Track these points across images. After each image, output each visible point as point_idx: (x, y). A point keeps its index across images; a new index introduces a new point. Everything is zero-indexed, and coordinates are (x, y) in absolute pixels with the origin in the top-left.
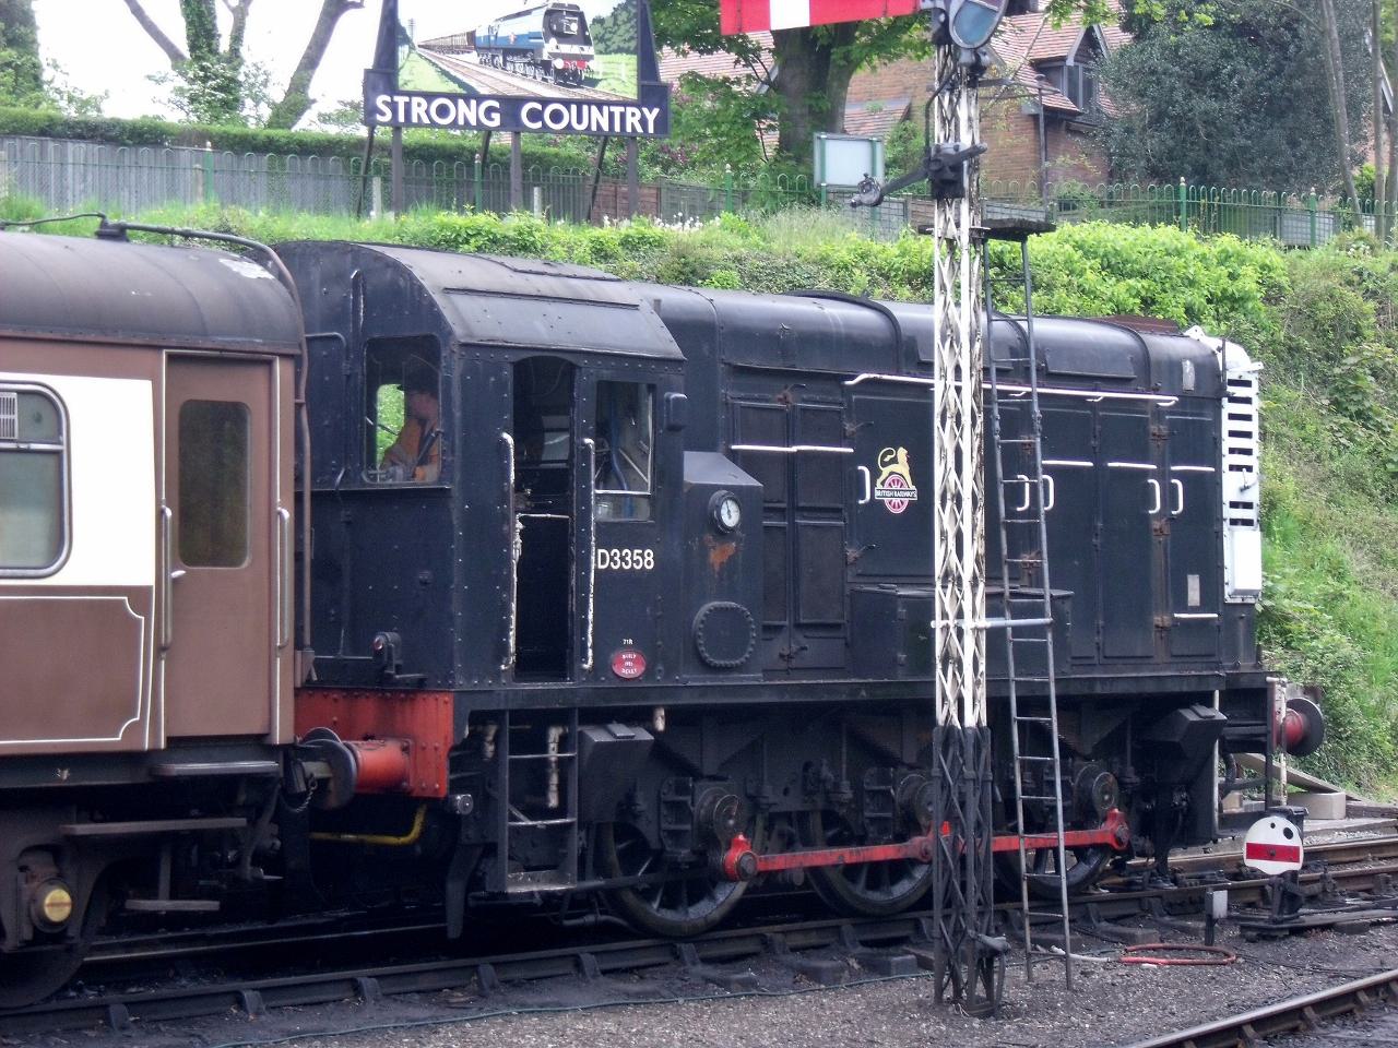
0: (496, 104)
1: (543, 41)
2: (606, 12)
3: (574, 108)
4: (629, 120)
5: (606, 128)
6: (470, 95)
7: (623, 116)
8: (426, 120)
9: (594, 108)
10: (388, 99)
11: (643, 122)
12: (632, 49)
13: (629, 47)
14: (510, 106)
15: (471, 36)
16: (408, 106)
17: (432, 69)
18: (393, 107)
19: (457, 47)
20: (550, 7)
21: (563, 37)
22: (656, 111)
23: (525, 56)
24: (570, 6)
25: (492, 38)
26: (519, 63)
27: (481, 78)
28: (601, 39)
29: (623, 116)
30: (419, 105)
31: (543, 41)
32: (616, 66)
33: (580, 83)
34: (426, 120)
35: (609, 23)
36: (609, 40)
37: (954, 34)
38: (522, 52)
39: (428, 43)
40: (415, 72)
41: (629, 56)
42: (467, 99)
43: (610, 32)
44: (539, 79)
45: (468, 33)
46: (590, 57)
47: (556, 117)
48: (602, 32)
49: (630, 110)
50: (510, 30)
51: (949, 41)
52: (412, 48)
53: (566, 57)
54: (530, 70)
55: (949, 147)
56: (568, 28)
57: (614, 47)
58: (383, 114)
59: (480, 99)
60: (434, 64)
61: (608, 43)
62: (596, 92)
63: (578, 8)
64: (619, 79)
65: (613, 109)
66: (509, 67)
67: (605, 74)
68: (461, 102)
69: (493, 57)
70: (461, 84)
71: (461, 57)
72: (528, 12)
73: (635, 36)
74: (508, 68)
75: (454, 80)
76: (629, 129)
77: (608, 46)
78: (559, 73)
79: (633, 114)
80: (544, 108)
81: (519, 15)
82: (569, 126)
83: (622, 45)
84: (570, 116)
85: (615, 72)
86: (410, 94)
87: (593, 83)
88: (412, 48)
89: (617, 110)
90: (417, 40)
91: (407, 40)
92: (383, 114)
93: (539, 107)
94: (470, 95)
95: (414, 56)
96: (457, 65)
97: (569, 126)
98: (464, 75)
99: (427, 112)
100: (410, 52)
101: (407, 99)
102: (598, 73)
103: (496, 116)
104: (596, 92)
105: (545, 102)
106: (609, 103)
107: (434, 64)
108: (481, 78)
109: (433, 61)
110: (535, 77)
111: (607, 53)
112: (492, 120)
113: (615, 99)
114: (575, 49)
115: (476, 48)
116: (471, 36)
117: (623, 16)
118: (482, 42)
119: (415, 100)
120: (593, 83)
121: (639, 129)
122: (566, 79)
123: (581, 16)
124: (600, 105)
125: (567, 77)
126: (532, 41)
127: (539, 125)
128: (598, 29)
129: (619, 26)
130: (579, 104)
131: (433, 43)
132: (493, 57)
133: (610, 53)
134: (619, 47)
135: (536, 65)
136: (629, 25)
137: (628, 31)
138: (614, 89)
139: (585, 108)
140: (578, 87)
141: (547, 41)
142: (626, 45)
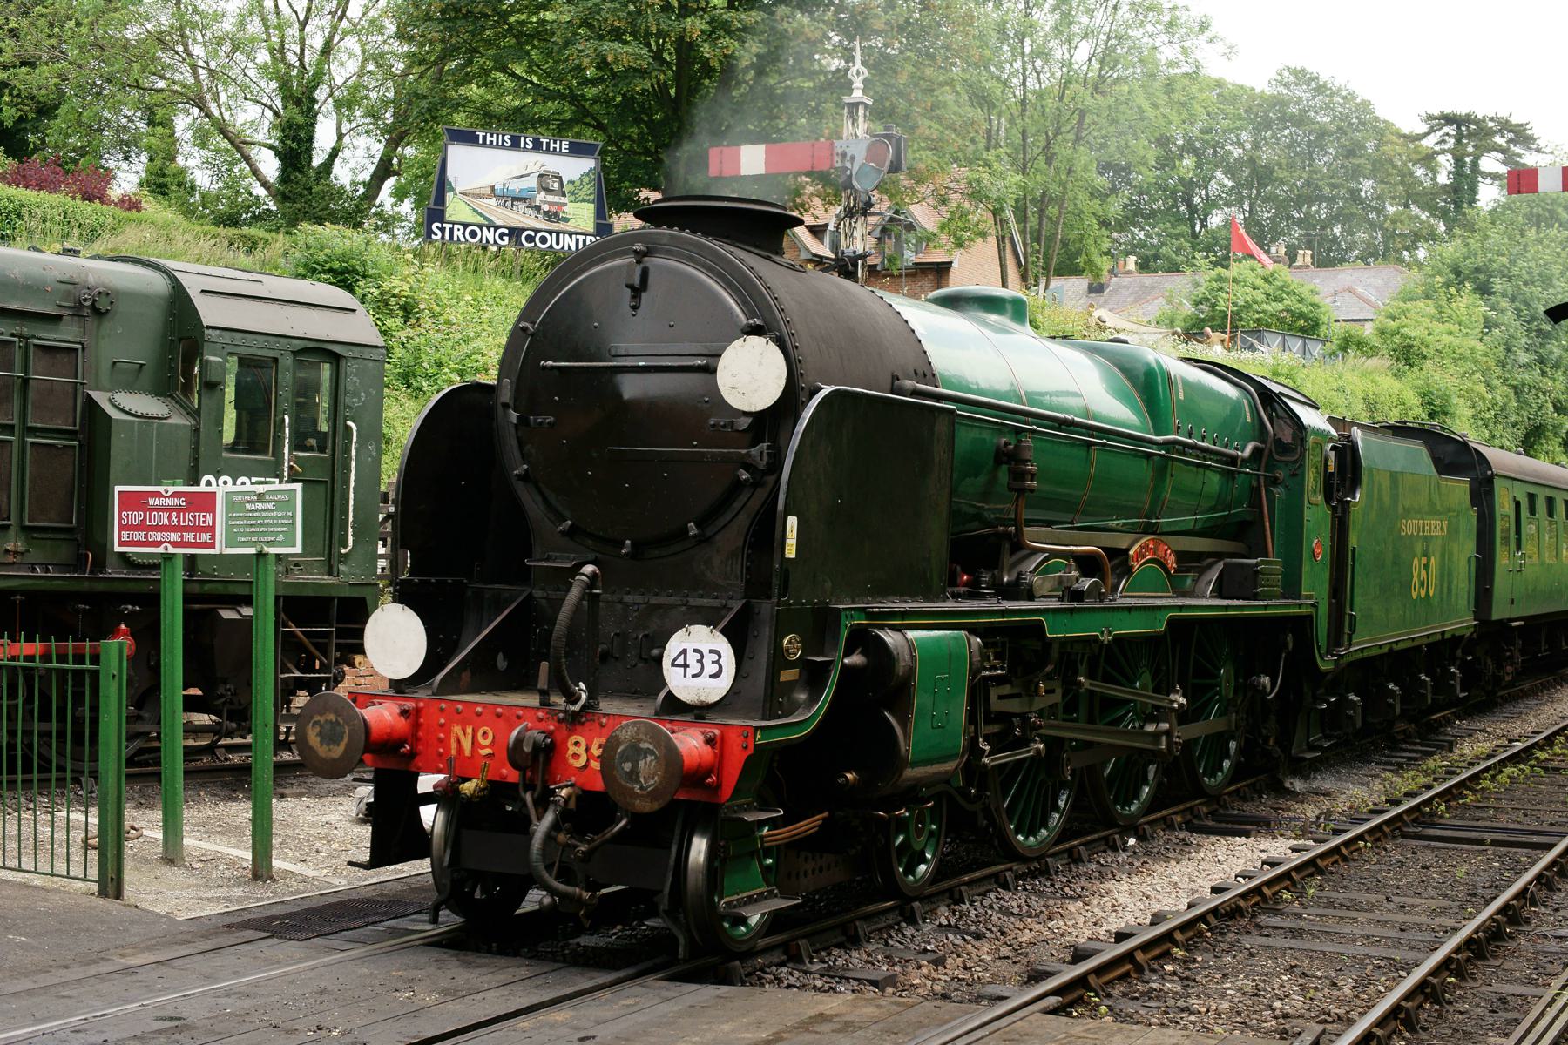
0: (506, 231)
2: (576, 178)
5: (573, 248)
6: (491, 226)
14: (515, 233)
15: (492, 188)
16: (452, 230)
18: (442, 230)
21: (548, 190)
26: (521, 206)
33: (558, 220)
34: (462, 239)
35: (578, 184)
37: (855, 183)
38: (524, 200)
40: (456, 209)
42: (489, 228)
47: (544, 240)
49: (589, 238)
50: (516, 187)
51: (852, 187)
53: (551, 204)
54: (528, 211)
55: (849, 252)
59: (496, 228)
70: (485, 218)
72: (528, 175)
78: (546, 213)
82: (551, 246)
84: (551, 240)
86: (454, 223)
87: (567, 220)
89: (581, 238)
90: (458, 190)
91: (452, 189)
94: (491, 226)
97: (551, 246)
103: (506, 238)
105: (537, 231)
114: (556, 199)
116: (492, 188)
117: (587, 180)
118: (498, 192)
119: (456, 227)
120: (567, 220)
123: (560, 178)
125: (551, 216)
130: (558, 233)
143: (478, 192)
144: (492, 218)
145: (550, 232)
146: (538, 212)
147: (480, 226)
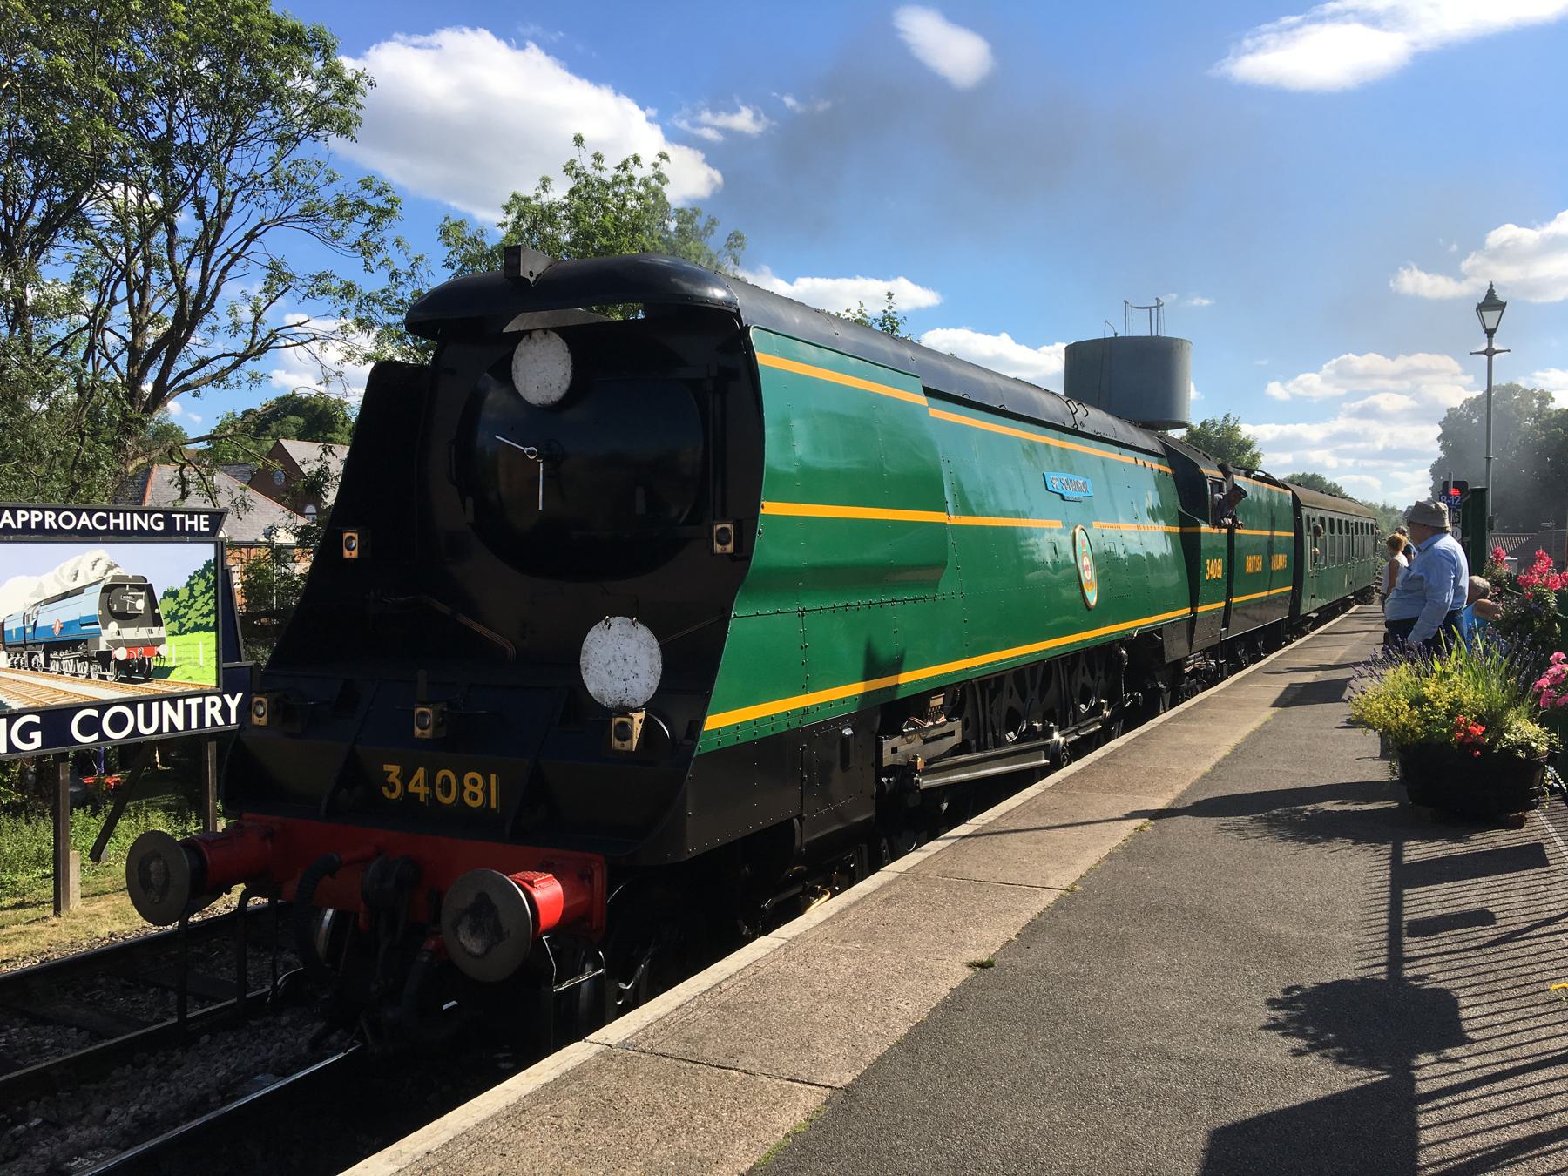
1: (100, 626)
2: (180, 583)
3: (140, 707)
4: (209, 711)
5: (180, 725)
7: (201, 707)
9: (166, 704)
11: (225, 711)
12: (211, 625)
13: (208, 623)
14: (54, 720)
20: (108, 581)
21: (125, 618)
22: (239, 696)
23: (76, 650)
25: (29, 631)
28: (174, 617)
29: (201, 707)
31: (100, 626)
32: (190, 648)
35: (184, 595)
36: (184, 616)
38: (72, 645)
43: (185, 607)
44: (95, 677)
46: (161, 641)
47: (118, 722)
49: (209, 700)
50: (54, 618)
53: (129, 644)
54: (83, 668)
56: (133, 607)
57: (191, 624)
61: (182, 620)
63: (146, 580)
64: (196, 664)
65: (188, 701)
66: (54, 666)
67: (178, 659)
69: (31, 656)
72: (79, 591)
74: (52, 668)
77: (182, 625)
78: (122, 666)
79: (213, 705)
80: (102, 715)
81: (66, 596)
83: (199, 621)
85: (192, 656)
87: (164, 672)
89: (194, 702)
93: (95, 713)
97: (135, 730)
102: (171, 659)
104: (168, 684)
105: (103, 706)
106: (185, 696)
108: (11, 687)
110: (89, 676)
111: (181, 634)
112: (32, 741)
114: (142, 633)
117: (201, 585)
120: (164, 672)
123: (149, 589)
124: (173, 700)
125: (134, 671)
126: (83, 628)
127: (95, 737)
130: (148, 703)
132: (31, 656)
133: (185, 633)
134: (195, 623)
135: (90, 660)
136: (207, 596)
137: (207, 603)
139: (155, 705)
141: (105, 627)
142: (204, 621)
146: (106, 667)
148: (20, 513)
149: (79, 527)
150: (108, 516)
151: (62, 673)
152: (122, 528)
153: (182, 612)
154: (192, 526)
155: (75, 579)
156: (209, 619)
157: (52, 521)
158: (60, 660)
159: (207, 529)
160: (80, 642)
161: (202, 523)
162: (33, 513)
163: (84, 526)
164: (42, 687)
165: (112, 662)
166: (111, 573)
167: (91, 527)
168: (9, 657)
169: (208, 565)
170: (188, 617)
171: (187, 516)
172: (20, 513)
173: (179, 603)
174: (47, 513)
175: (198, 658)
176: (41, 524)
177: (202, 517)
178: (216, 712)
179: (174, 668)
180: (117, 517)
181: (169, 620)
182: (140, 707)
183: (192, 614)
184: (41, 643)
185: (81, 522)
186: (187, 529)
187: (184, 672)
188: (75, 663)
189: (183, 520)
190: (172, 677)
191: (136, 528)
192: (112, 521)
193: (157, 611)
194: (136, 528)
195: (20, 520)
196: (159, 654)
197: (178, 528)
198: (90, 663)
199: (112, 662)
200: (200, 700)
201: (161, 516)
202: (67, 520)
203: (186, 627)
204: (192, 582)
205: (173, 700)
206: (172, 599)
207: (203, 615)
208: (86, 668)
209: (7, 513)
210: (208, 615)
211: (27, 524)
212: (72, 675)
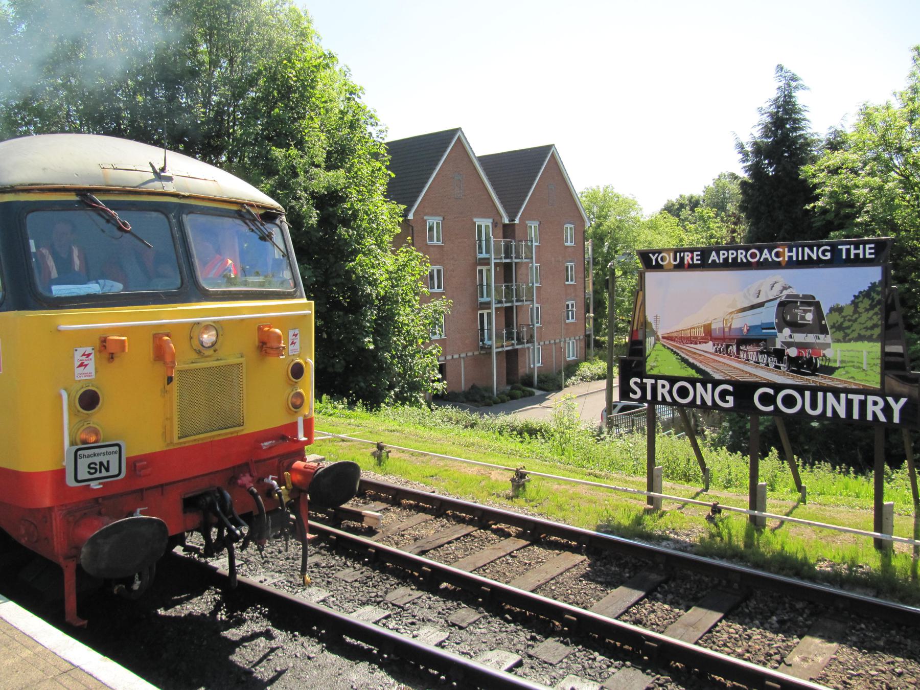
0: (730, 388)
2: (845, 300)
3: (807, 394)
4: (870, 408)
5: (842, 414)
6: (706, 380)
7: (863, 404)
8: (669, 399)
9: (829, 395)
10: (638, 380)
11: (887, 410)
12: (875, 337)
13: (872, 335)
17: (674, 357)
19: (695, 338)
20: (783, 299)
21: (796, 326)
24: (805, 296)
25: (726, 330)
26: (752, 351)
27: (715, 364)
28: (839, 328)
29: (863, 404)
30: (663, 386)
31: (776, 331)
34: (669, 399)
35: (849, 311)
36: (848, 328)
39: (670, 335)
41: (871, 344)
43: (849, 320)
44: (771, 367)
45: (705, 326)
47: (789, 401)
48: (841, 320)
49: (870, 399)
50: (742, 323)
52: (657, 339)
53: (800, 346)
54: (763, 358)
56: (803, 318)
57: (855, 335)
58: (635, 393)
59: (716, 383)
60: (675, 353)
61: (847, 331)
62: (832, 379)
63: (814, 298)
64: (859, 367)
65: (850, 396)
66: (743, 355)
67: (842, 362)
68: (698, 385)
70: (699, 370)
71: (698, 346)
72: (761, 305)
73: (879, 323)
74: (741, 356)
75: (693, 366)
76: (870, 417)
77: (846, 335)
78: (792, 361)
80: (776, 393)
81: (753, 307)
83: (863, 333)
86: (656, 378)
87: (830, 370)
88: (657, 339)
89: (856, 398)
90: (660, 334)
91: (654, 333)
92: (635, 393)
93: (771, 391)
95: (658, 346)
96: (695, 353)
98: (701, 362)
99: (670, 392)
100: (655, 343)
101: (653, 381)
103: (730, 398)
104: (832, 379)
105: (778, 388)
106: (847, 391)
107: (675, 353)
108: (715, 364)
109: (674, 350)
110: (767, 365)
111: (845, 342)
112: (727, 402)
113: (854, 387)
114: (810, 338)
115: (713, 339)
117: (867, 303)
118: (717, 334)
119: (660, 382)
121: (882, 418)
122: (800, 366)
123: (817, 305)
124: (836, 392)
126: (764, 331)
127: (771, 408)
128: (836, 317)
129: (860, 313)
130: (814, 390)
131: (674, 335)
132: (728, 346)
133: (849, 341)
134: (859, 335)
135: (769, 354)
136: (871, 312)
137: (871, 318)
138: (853, 378)
139: (820, 395)
140: (813, 374)
141: (780, 331)
142: (869, 333)
143: (687, 334)
144: (708, 370)
145: (801, 389)
146: (780, 360)
147: (693, 382)
148: (722, 252)
149: (761, 260)
150: (784, 251)
151: (748, 360)
152: (795, 259)
153: (846, 324)
154: (857, 255)
155: (758, 297)
156: (873, 332)
157: (743, 256)
158: (746, 352)
159: (699, 262)
160: (760, 340)
161: (868, 251)
162: (730, 252)
163: (766, 259)
164: (735, 368)
165: (786, 358)
166: (785, 292)
167: (770, 260)
168: (714, 345)
169: (873, 287)
170: (853, 328)
171: (852, 247)
172: (722, 252)
173: (844, 317)
174: (739, 251)
175: (861, 363)
176: (735, 259)
177: (867, 246)
178: (878, 409)
179: (839, 368)
180: (790, 251)
181: (834, 330)
182: (807, 394)
183: (856, 326)
184: (734, 339)
185: (764, 256)
186: (852, 257)
187: (847, 372)
188: (757, 354)
189: (848, 251)
190: (835, 375)
191: (806, 258)
192: (787, 254)
193: (823, 322)
194: (806, 258)
195: (722, 257)
196: (824, 356)
197: (844, 257)
198: (768, 356)
199: (786, 358)
200: (862, 397)
201: (828, 248)
202: (753, 256)
203: (850, 337)
204: (857, 301)
205: (836, 392)
206: (837, 313)
207: (867, 329)
208: (765, 359)
209: (714, 253)
210: (872, 328)
211: (726, 259)
212: (755, 362)
